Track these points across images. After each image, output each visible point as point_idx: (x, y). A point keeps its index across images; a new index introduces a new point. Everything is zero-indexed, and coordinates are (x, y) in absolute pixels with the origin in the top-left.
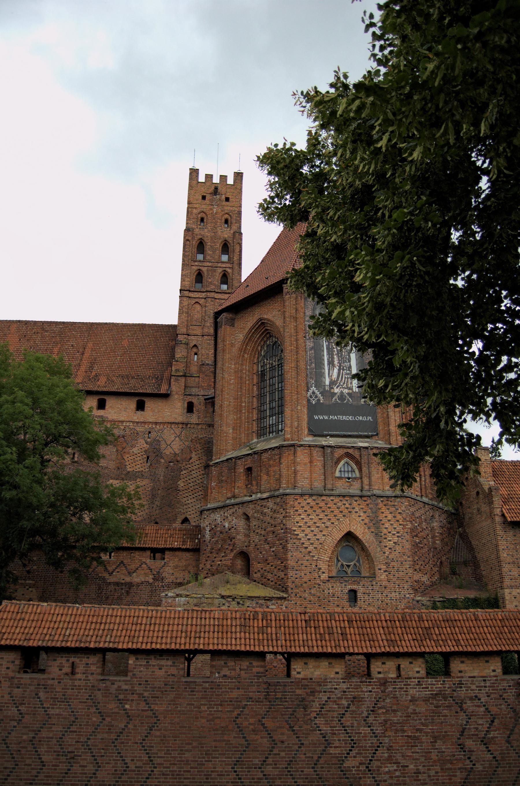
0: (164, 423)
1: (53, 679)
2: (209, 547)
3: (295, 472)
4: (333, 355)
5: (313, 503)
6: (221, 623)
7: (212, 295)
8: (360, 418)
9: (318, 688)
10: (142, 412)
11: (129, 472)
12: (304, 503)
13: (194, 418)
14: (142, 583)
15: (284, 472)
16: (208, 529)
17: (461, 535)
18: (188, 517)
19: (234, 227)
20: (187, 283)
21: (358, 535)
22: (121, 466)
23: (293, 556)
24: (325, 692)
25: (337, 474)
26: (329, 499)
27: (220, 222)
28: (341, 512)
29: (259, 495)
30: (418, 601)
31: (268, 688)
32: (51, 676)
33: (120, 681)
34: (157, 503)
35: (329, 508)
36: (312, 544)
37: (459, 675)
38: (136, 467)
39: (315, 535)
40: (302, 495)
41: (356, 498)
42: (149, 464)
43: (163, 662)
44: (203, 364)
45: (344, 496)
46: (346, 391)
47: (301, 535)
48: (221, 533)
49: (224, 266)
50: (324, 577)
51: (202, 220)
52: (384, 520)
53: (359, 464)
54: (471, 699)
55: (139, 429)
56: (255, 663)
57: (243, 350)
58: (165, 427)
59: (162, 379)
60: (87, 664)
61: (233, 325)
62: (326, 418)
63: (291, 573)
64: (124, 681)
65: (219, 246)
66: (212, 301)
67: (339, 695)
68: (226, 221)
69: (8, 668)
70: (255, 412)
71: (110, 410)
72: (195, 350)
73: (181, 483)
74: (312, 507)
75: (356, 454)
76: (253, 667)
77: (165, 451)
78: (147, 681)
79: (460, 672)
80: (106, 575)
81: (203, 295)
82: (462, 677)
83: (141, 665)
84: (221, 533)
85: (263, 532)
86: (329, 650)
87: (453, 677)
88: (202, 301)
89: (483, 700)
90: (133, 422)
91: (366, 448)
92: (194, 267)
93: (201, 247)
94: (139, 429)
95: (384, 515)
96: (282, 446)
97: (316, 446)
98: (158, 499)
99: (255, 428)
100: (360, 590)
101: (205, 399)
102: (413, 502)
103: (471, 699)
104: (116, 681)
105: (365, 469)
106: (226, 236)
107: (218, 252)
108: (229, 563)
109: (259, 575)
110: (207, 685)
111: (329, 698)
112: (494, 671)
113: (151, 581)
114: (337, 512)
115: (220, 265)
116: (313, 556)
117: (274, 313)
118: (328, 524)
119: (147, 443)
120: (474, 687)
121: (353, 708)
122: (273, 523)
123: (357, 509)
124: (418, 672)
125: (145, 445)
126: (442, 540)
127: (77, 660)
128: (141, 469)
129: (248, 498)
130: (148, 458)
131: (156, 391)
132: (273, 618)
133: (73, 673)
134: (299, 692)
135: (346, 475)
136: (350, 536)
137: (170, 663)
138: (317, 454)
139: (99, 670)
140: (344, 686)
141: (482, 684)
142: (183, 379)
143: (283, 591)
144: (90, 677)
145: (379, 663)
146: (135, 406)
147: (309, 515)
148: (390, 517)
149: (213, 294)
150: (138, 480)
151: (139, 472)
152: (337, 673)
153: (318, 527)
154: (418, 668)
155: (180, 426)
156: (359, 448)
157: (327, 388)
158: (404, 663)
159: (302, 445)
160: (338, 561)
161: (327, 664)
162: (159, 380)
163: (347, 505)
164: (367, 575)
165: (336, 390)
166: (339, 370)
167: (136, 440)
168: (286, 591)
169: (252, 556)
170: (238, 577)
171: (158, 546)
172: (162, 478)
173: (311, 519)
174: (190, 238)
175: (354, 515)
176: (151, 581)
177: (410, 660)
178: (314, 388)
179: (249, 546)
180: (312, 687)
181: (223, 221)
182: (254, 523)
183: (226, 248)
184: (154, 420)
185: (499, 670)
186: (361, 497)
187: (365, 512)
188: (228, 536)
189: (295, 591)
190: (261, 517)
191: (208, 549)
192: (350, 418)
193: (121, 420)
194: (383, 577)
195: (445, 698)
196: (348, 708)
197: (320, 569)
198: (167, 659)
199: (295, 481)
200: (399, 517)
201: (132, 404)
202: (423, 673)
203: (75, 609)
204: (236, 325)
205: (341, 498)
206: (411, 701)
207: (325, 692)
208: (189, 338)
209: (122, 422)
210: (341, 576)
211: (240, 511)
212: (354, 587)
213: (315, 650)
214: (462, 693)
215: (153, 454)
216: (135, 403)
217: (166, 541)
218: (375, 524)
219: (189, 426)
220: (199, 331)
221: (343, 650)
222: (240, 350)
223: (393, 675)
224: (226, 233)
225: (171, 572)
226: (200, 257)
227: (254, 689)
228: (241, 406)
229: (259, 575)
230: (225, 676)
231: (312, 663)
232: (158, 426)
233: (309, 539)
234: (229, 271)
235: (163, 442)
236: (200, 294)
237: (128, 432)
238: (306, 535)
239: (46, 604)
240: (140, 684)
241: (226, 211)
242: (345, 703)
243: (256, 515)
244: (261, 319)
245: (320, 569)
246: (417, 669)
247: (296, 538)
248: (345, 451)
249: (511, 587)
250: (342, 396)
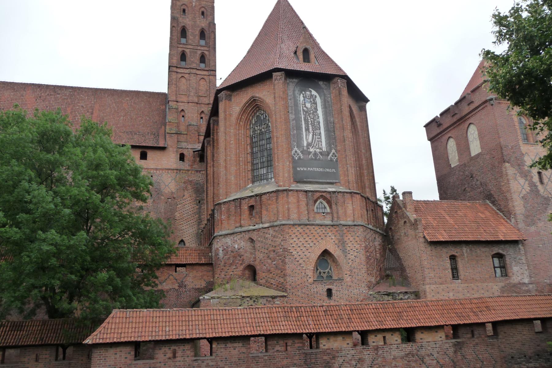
1: (160, 362)
2: (223, 262)
3: (288, 209)
4: (308, 124)
5: (301, 231)
6: (270, 316)
7: (194, 71)
8: (328, 170)
9: (337, 355)
10: (145, 161)
12: (295, 231)
13: (185, 165)
14: (170, 289)
15: (280, 208)
16: (221, 249)
17: (390, 250)
18: (184, 239)
19: (210, 19)
20: (175, 61)
21: (331, 251)
23: (290, 267)
24: (341, 356)
25: (315, 210)
26: (312, 227)
27: (198, 14)
28: (320, 236)
29: (261, 226)
30: (371, 295)
31: (306, 357)
32: (159, 361)
33: (207, 360)
35: (312, 233)
36: (302, 258)
37: (421, 341)
39: (304, 252)
40: (294, 225)
41: (329, 227)
43: (236, 345)
44: (190, 125)
45: (321, 225)
46: (318, 150)
47: (294, 253)
48: (232, 252)
50: (311, 280)
51: (184, 11)
52: (348, 241)
53: (329, 203)
54: (428, 356)
56: (296, 341)
57: (239, 119)
59: (158, 135)
60: (184, 350)
61: (230, 100)
62: (305, 169)
63: (288, 279)
64: (210, 359)
65: (197, 33)
66: (194, 76)
67: (350, 358)
68: (203, 13)
69: (126, 358)
70: (250, 164)
72: (182, 114)
73: (177, 215)
74: (300, 233)
75: (328, 196)
76: (295, 343)
78: (226, 358)
79: (421, 339)
81: (187, 71)
82: (422, 342)
83: (221, 348)
84: (232, 252)
85: (266, 251)
86: (344, 330)
87: (418, 343)
88: (186, 76)
89: (435, 356)
91: (334, 192)
92: (179, 49)
95: (348, 238)
96: (277, 191)
97: (301, 191)
99: (250, 177)
100: (334, 288)
101: (194, 152)
102: (365, 229)
103: (428, 356)
104: (205, 360)
105: (334, 206)
106: (203, 25)
107: (198, 37)
108: (240, 273)
109: (264, 281)
110: (266, 358)
111: (344, 360)
112: (441, 337)
113: (177, 288)
114: (317, 236)
115: (199, 48)
116: (303, 267)
117: (264, 93)
118: (312, 244)
120: (429, 348)
121: (359, 366)
122: (274, 244)
123: (330, 234)
124: (396, 340)
126: (380, 253)
127: (176, 348)
129: (252, 228)
131: (156, 145)
132: (303, 311)
133: (174, 356)
134: (325, 358)
135: (321, 211)
136: (326, 253)
137: (241, 345)
138: (302, 196)
139: (193, 354)
140: (353, 352)
141: (435, 346)
142: (176, 136)
143: (283, 292)
144: (187, 359)
145: (373, 336)
146: (139, 156)
147: (299, 239)
148: (351, 239)
149: (195, 70)
152: (348, 344)
153: (305, 247)
154: (396, 338)
155: (175, 171)
156: (330, 192)
157: (305, 148)
158: (388, 336)
159: (292, 190)
160: (317, 269)
161: (341, 338)
162: (157, 136)
163: (324, 232)
164: (336, 278)
165: (312, 150)
166: (313, 135)
168: (286, 291)
169: (258, 268)
170: (248, 283)
171: (181, 263)
172: (163, 210)
173: (301, 241)
174: (175, 25)
175: (328, 239)
176: (177, 288)
177: (392, 333)
178: (296, 149)
179: (255, 261)
180: (333, 354)
181: (201, 13)
182: (258, 245)
183: (202, 35)
185: (444, 337)
186: (332, 226)
187: (335, 236)
188: (237, 255)
189: (291, 291)
190: (264, 241)
191: (222, 264)
192: (321, 169)
194: (348, 280)
195: (413, 356)
196: (356, 366)
197: (308, 275)
198: (239, 343)
199: (289, 216)
200: (357, 239)
202: (399, 341)
203: (168, 312)
204: (233, 100)
205: (319, 227)
206: (393, 359)
207: (341, 356)
208: (178, 104)
210: (320, 278)
211: (247, 236)
212: (330, 287)
213: (335, 330)
214: (423, 352)
217: (186, 259)
218: (342, 243)
219: (181, 172)
220: (184, 99)
221: (352, 329)
222: (237, 119)
223: (382, 343)
224: (203, 23)
225: (191, 280)
226: (183, 40)
227: (297, 358)
228: (239, 160)
229: (264, 281)
230: (278, 351)
231: (332, 339)
233: (300, 255)
234: (206, 53)
236: (184, 70)
238: (298, 253)
239: (146, 310)
240: (222, 361)
241: (203, 5)
242: (354, 363)
243: (259, 239)
244: (253, 97)
245: (308, 275)
246: (396, 339)
247: (291, 255)
248: (321, 194)
249: (430, 284)
250: (315, 154)
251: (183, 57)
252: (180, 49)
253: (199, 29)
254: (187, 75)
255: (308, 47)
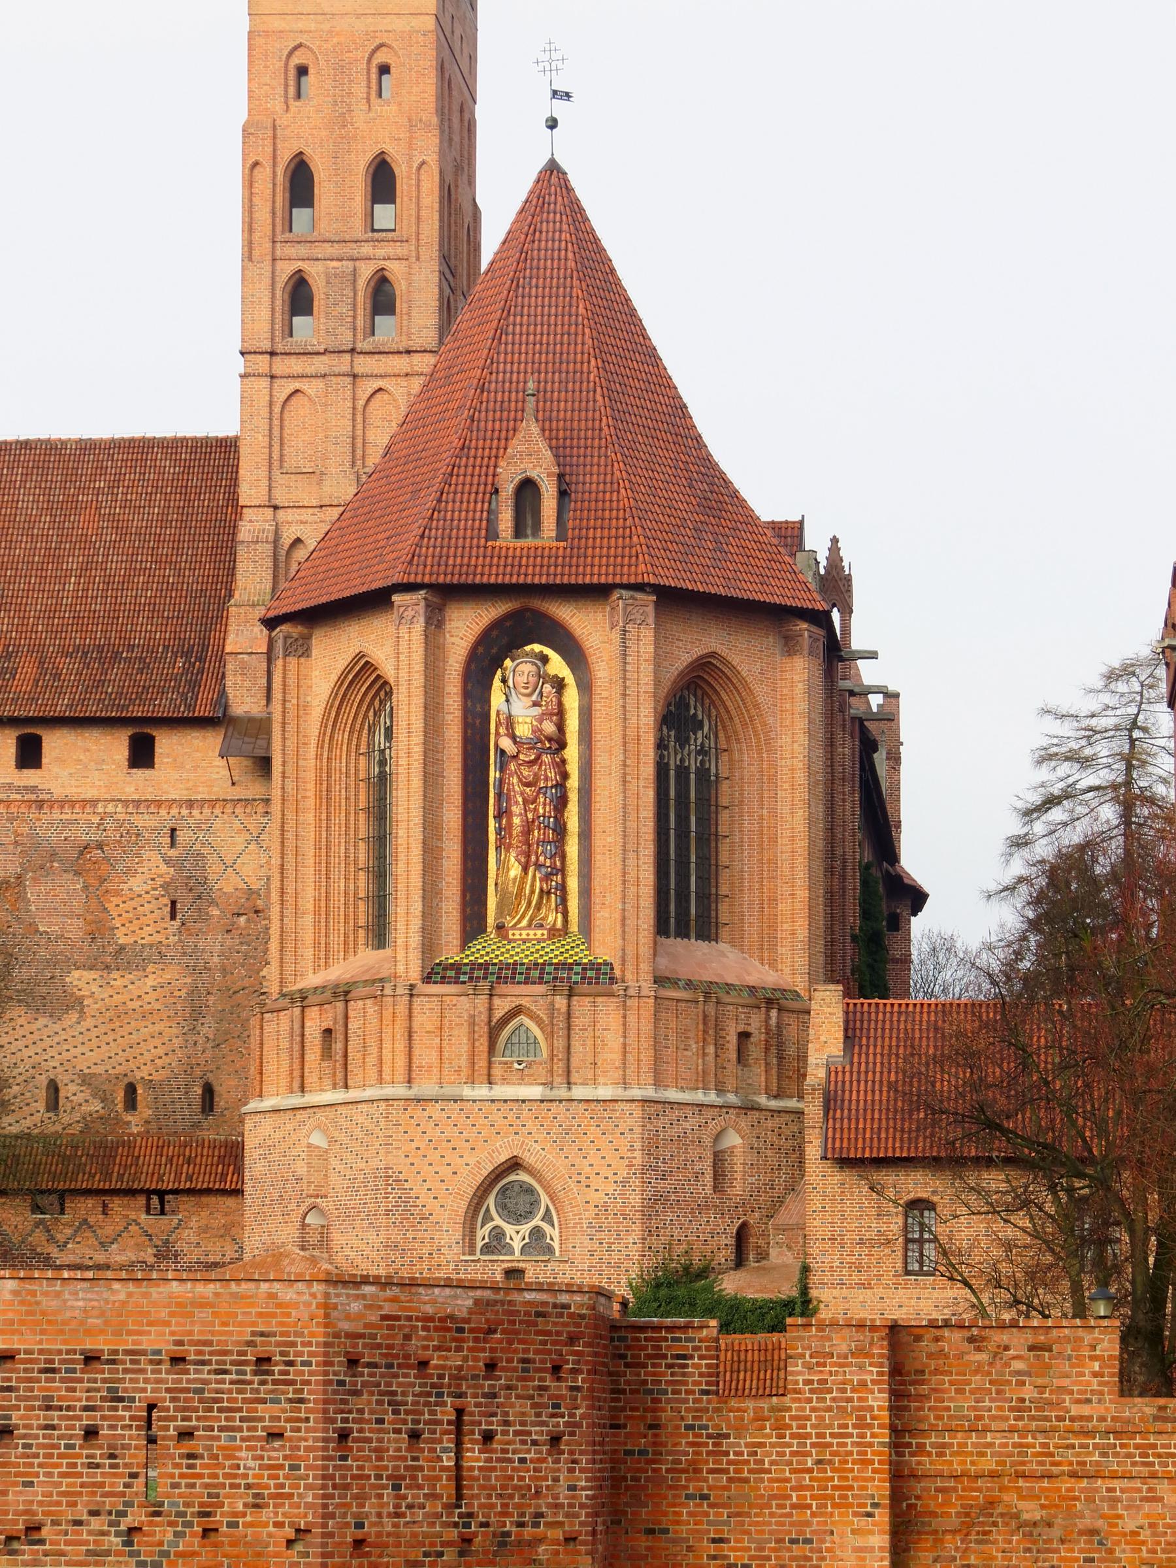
0: (213, 803)
10: (148, 772)
11: (123, 948)
22: (98, 930)
34: (205, 1030)
38: (144, 933)
42: (177, 923)
49: (381, 253)
55: (144, 820)
58: (217, 811)
59: (201, 659)
61: (307, 653)
71: (56, 769)
77: (222, 883)
80: (54, 1252)
90: (126, 803)
93: (300, 184)
94: (144, 820)
98: (208, 1019)
115: (367, 249)
119: (168, 862)
125: (163, 868)
128: (157, 938)
130: (173, 903)
146: (126, 753)
150: (150, 969)
151: (151, 946)
167: (138, 855)
172: (216, 959)
184: (184, 795)
193: (88, 796)
201: (114, 747)
209: (94, 803)
215: (186, 898)
216: (126, 743)
217: (178, 1174)
232: (195, 812)
235: (212, 859)
237: (112, 833)
244: (360, 655)
251: (299, 297)
252: (286, 270)
253: (369, 157)
254: (319, 384)
255: (533, 474)
